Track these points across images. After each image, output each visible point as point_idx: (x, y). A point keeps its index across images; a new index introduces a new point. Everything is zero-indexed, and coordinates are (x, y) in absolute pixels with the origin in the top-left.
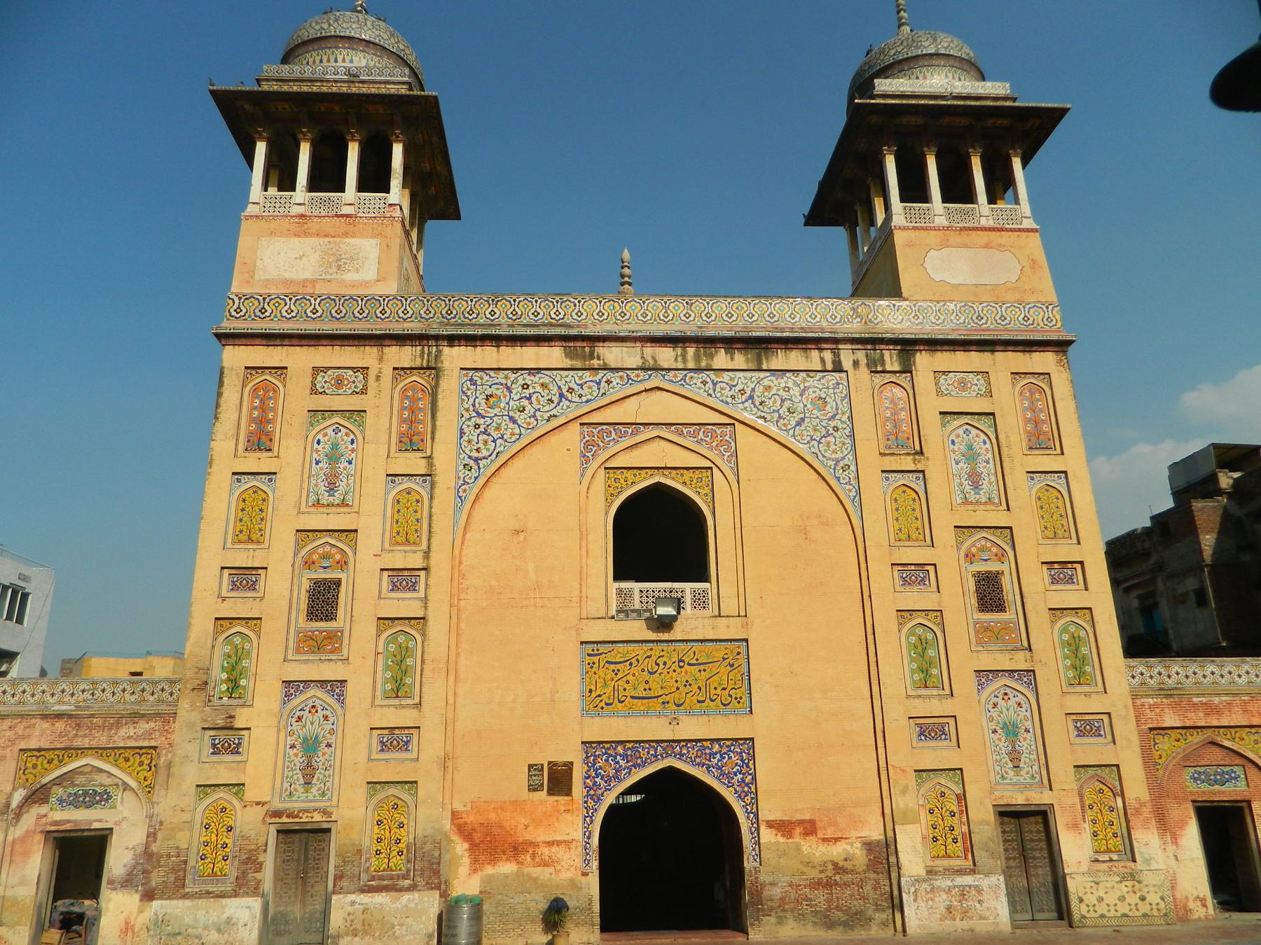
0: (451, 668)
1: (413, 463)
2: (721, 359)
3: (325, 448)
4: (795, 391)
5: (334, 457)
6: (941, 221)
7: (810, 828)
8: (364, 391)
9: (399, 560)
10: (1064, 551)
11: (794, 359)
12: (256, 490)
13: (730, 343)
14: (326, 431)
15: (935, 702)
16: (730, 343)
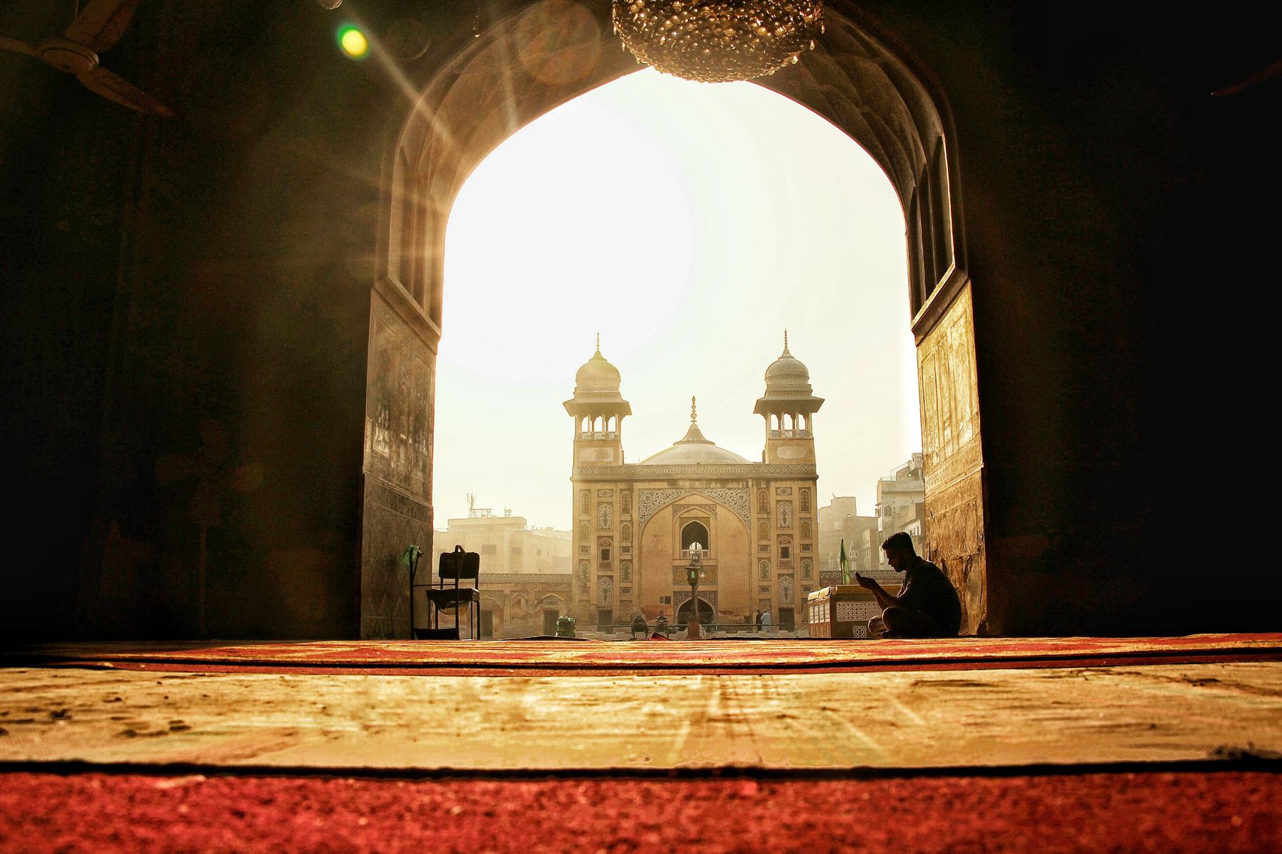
0: (640, 573)
1: (626, 517)
2: (713, 485)
3: (602, 512)
4: (734, 494)
5: (605, 515)
6: (783, 436)
7: (731, 613)
8: (612, 496)
9: (624, 544)
10: (807, 541)
11: (735, 485)
12: (585, 525)
13: (716, 480)
14: (603, 509)
15: (766, 582)
16: (716, 480)
